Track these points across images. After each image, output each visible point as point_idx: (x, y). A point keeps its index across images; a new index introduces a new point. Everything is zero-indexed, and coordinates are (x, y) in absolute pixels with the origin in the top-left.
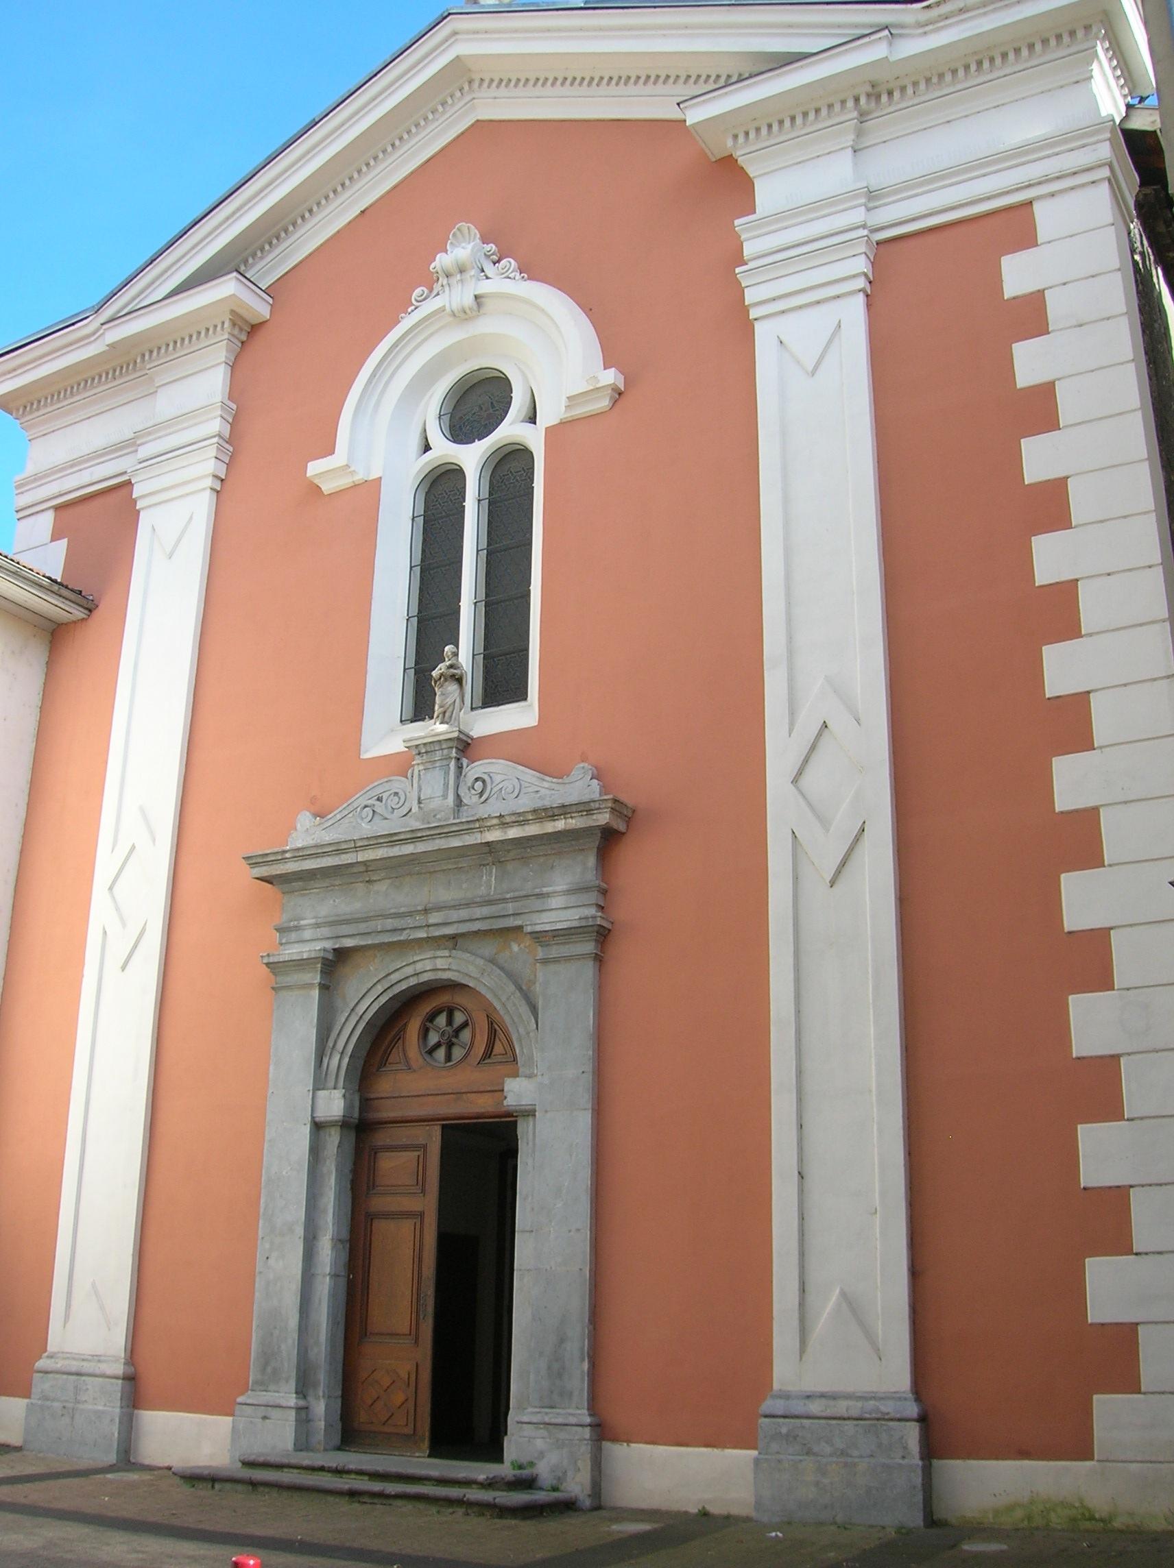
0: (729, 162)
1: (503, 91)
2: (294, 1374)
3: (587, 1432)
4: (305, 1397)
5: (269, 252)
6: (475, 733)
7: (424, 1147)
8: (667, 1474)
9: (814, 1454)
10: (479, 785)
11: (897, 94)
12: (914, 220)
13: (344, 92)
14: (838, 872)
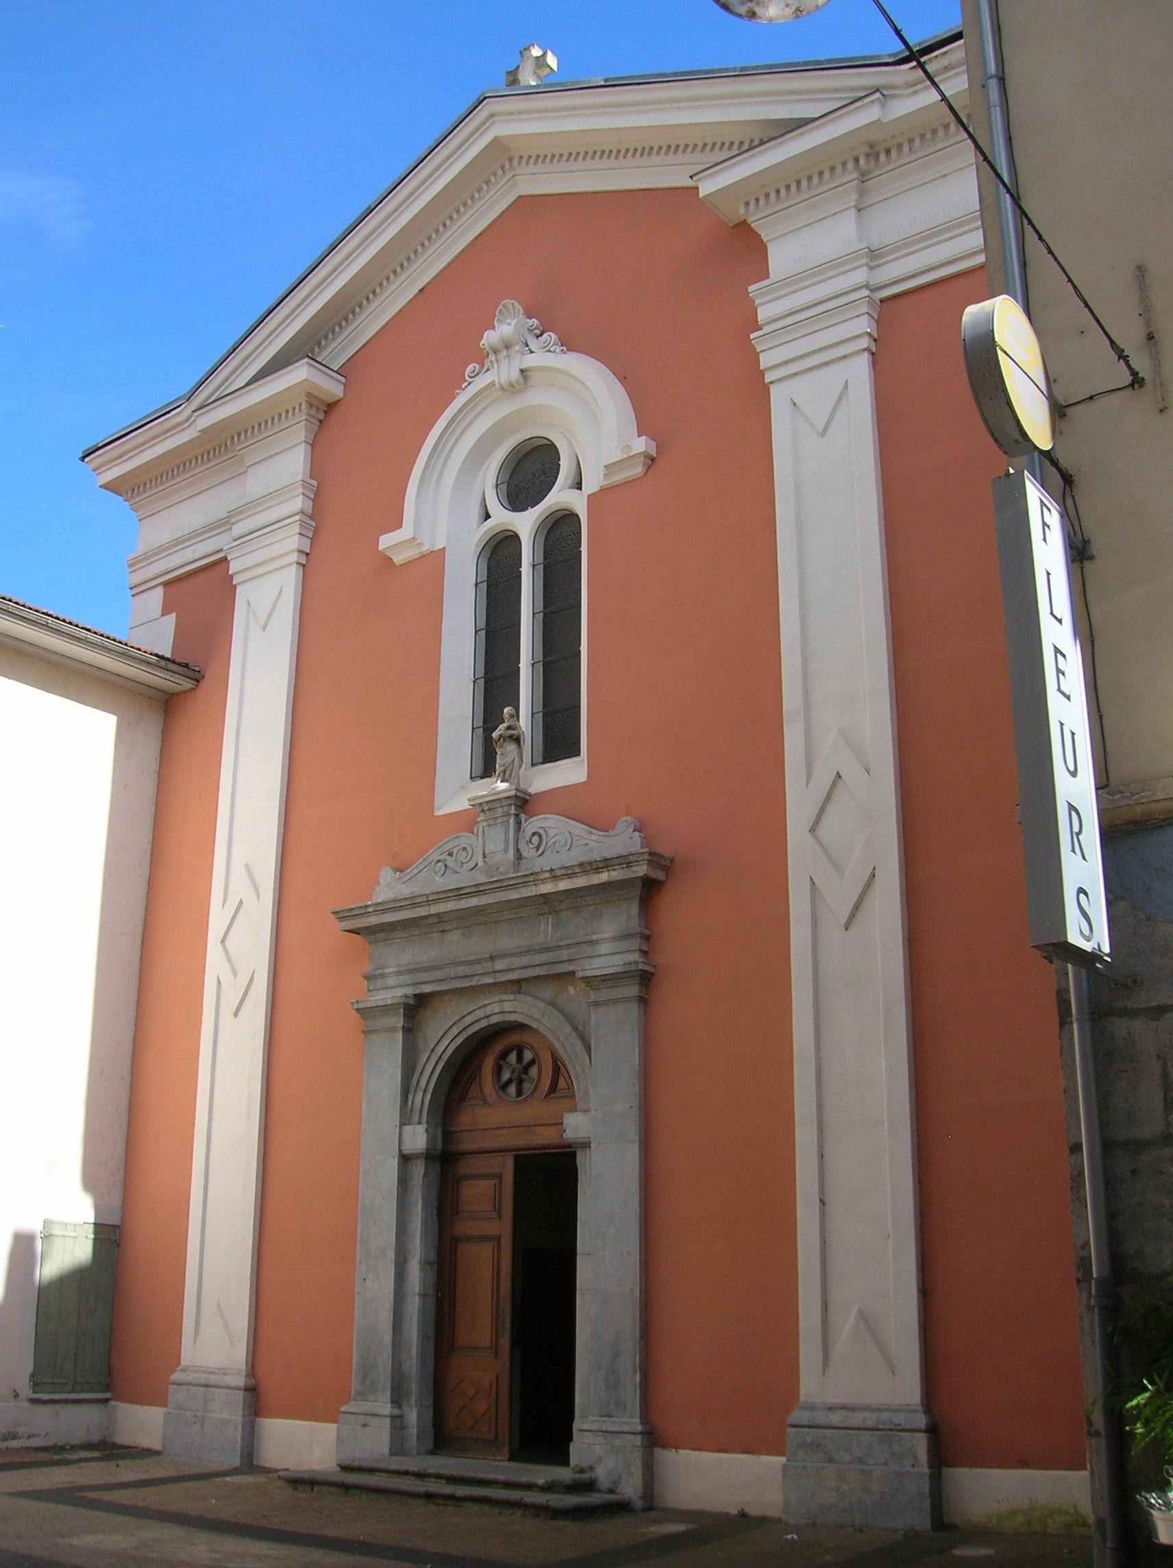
0: (743, 226)
1: (540, 167)
2: (389, 1386)
3: (638, 1440)
4: (400, 1407)
5: (340, 333)
6: (533, 790)
7: (499, 1176)
8: (714, 1478)
9: (835, 1461)
10: (536, 839)
11: (894, 153)
12: (913, 276)
13: (396, 179)
14: (852, 915)
